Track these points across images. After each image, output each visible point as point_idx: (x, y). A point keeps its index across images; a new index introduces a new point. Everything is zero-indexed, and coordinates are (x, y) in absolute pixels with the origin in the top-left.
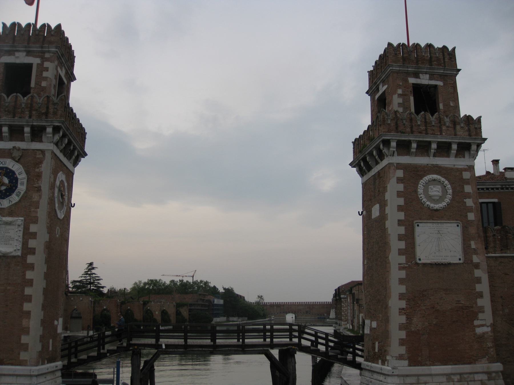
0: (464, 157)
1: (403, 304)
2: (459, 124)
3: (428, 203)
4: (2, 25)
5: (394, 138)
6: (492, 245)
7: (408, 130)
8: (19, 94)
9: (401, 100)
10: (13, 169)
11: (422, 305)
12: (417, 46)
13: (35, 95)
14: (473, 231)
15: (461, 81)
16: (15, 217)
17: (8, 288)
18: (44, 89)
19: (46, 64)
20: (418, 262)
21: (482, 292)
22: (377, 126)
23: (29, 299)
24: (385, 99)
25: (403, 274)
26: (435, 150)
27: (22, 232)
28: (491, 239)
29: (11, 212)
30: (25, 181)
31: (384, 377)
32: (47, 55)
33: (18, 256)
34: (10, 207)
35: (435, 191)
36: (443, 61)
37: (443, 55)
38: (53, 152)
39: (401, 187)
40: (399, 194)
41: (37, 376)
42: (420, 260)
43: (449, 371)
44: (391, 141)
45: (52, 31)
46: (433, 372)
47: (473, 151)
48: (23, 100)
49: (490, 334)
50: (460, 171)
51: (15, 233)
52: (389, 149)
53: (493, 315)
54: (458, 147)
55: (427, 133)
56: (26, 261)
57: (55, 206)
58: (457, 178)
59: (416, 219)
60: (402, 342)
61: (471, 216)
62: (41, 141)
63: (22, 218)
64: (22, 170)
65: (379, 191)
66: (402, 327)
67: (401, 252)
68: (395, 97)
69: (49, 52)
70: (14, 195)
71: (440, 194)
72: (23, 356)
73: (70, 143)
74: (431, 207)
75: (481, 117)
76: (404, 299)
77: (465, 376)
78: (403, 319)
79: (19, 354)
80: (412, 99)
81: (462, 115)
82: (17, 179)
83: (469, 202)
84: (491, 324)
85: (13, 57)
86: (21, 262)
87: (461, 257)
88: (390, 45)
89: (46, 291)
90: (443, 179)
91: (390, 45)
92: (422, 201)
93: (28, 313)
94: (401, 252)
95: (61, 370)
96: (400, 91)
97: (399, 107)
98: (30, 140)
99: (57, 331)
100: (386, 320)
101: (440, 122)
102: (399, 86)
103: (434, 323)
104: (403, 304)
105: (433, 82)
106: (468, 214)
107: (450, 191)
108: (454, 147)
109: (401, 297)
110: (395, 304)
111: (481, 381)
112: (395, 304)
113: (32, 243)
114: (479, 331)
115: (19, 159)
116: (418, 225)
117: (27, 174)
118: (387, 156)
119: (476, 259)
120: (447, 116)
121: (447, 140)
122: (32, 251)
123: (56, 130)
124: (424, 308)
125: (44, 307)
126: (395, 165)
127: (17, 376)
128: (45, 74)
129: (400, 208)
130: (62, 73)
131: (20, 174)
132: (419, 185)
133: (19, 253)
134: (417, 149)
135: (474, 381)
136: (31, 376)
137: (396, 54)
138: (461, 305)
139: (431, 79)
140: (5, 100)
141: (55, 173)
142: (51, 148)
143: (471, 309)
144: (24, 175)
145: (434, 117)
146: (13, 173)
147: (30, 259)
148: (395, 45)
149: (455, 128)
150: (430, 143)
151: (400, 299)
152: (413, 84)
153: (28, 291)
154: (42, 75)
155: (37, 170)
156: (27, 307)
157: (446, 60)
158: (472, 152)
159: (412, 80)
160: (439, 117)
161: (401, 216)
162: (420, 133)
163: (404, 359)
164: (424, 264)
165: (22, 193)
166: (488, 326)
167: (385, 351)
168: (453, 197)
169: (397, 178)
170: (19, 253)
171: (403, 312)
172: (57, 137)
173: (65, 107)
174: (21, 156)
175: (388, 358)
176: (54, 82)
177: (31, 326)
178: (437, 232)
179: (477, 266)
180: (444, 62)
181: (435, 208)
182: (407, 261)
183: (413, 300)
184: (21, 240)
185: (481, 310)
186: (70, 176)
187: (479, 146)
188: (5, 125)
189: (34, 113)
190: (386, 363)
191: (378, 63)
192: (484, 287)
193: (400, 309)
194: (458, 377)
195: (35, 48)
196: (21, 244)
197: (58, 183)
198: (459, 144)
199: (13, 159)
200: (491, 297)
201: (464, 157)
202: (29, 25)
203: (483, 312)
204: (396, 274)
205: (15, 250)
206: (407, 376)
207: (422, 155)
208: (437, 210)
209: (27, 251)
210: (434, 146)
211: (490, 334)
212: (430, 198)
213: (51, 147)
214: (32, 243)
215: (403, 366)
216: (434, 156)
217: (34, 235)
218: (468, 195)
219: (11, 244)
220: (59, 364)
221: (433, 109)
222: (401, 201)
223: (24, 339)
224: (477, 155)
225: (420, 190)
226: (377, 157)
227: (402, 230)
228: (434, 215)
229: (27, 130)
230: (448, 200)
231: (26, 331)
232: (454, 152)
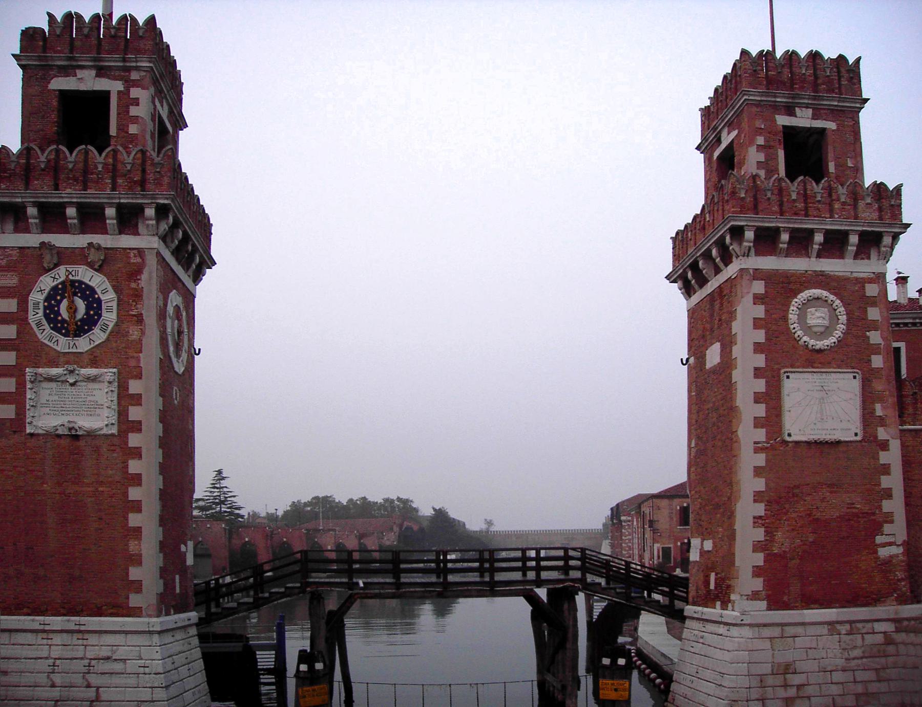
0: (869, 258)
1: (760, 509)
2: (863, 199)
3: (805, 338)
4: (47, 18)
5: (750, 223)
6: (911, 410)
7: (776, 208)
8: (90, 147)
9: (761, 157)
10: (90, 284)
11: (791, 510)
12: (791, 56)
13: (120, 148)
15: (868, 120)
16: (101, 367)
17: (100, 489)
20: (788, 439)
21: (890, 489)
22: (721, 203)
23: (137, 507)
24: (733, 156)
25: (760, 460)
26: (820, 244)
27: (115, 394)
28: (909, 400)
29: (94, 358)
30: (114, 304)
31: (727, 628)
32: (134, 76)
33: (113, 435)
34: (91, 351)
36: (834, 82)
37: (839, 72)
38: (158, 254)
39: (760, 311)
40: (757, 324)
41: (159, 633)
42: (789, 435)
43: (834, 619)
44: (746, 228)
45: (139, 28)
46: (807, 620)
47: (885, 247)
48: (99, 159)
49: (901, 558)
50: (862, 282)
52: (740, 244)
53: (907, 528)
54: (859, 240)
55: (806, 215)
56: (126, 443)
57: (168, 350)
58: (855, 296)
59: (787, 367)
60: (757, 572)
61: (877, 361)
62: (136, 233)
63: (115, 370)
64: (108, 285)
65: (720, 320)
66: (758, 547)
67: (758, 423)
68: (752, 150)
69: (137, 68)
70: (96, 330)
71: (826, 323)
72: (135, 600)
74: (810, 346)
75: (901, 185)
76: (761, 502)
77: (860, 625)
78: (760, 534)
79: (128, 598)
80: (781, 154)
81: (868, 182)
82: (99, 301)
83: (875, 337)
84: (904, 541)
85: (72, 79)
86: (119, 443)
87: (858, 431)
88: (744, 53)
89: (163, 494)
90: (832, 297)
91: (744, 53)
92: (796, 335)
93: (138, 530)
94: (758, 423)
95: (197, 625)
96: (760, 140)
97: (758, 168)
98: (117, 231)
99: (185, 562)
100: (732, 537)
101: (830, 195)
102: (759, 132)
103: (811, 540)
104: (760, 509)
105: (818, 124)
106: (873, 356)
107: (843, 318)
108: (854, 239)
109: (758, 497)
110: (747, 510)
111: (884, 633)
112: (747, 510)
113: (134, 413)
114: (883, 552)
115: (100, 266)
116: (788, 377)
117: (116, 292)
118: (737, 257)
119: (882, 434)
120: (842, 185)
121: (843, 228)
122: (137, 427)
123: (162, 211)
124: (794, 515)
125: (162, 521)
126: (751, 272)
127: (126, 633)
128: (134, 111)
129: (758, 348)
131: (105, 292)
132: (792, 308)
133: (114, 430)
134: (789, 243)
135: (874, 633)
136: (150, 633)
137: (755, 71)
138: (854, 510)
139: (815, 117)
140: (66, 158)
141: (164, 291)
142: (156, 246)
143: (873, 517)
144: (111, 295)
145: (821, 185)
146: (93, 290)
147: (134, 440)
148: (754, 53)
149: (855, 206)
150: (811, 232)
151: (755, 501)
152: (784, 126)
153: (134, 493)
154: (128, 112)
155: (133, 285)
156: (134, 520)
157: (844, 82)
158: (883, 249)
159: (783, 120)
160: (830, 186)
161: (760, 361)
162: (796, 214)
163: (759, 599)
164: (797, 443)
165: (111, 325)
166: (898, 545)
167: (729, 587)
168: (848, 329)
169: (754, 294)
170: (114, 430)
171: (760, 521)
172: (164, 227)
173: (175, 170)
174: (103, 261)
175: (733, 597)
176: (150, 126)
177: (144, 552)
178: (820, 388)
179: (884, 446)
180: (840, 84)
181: (817, 347)
182: (769, 436)
183: (778, 503)
184: (116, 407)
185: (889, 518)
187: (895, 237)
188: (71, 204)
190: (730, 605)
191: (720, 91)
192: (894, 481)
193: (754, 518)
194: (847, 627)
195: (113, 61)
196: (116, 414)
198: (862, 235)
199: (91, 265)
200: (906, 497)
201: (869, 258)
202: (96, 17)
203: (892, 522)
204: (749, 459)
205: (107, 425)
206: (765, 625)
208: (820, 351)
209: (127, 426)
210: (819, 238)
211: (901, 558)
212: (808, 329)
213: (155, 243)
214: (134, 413)
215: (759, 610)
216: (819, 256)
217: (137, 400)
218: (874, 326)
219: (99, 415)
220: (193, 616)
221: (817, 172)
222: (760, 336)
223: (134, 573)
224: (891, 255)
225: (793, 317)
226: (718, 260)
227: (760, 385)
228: (815, 360)
229: (110, 212)
230: (840, 334)
231: (137, 560)
232: (852, 249)
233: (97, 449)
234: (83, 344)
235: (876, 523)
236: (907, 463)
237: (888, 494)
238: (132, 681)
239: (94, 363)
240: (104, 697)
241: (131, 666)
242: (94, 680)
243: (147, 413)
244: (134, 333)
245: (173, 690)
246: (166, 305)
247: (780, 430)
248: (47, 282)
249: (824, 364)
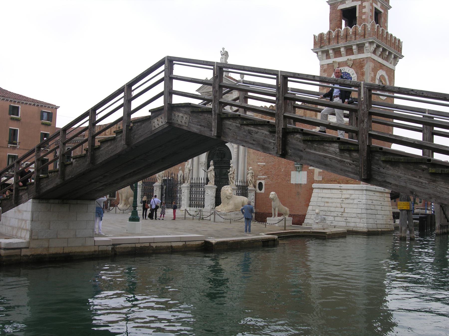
18: (364, 20)
62: (363, 53)
73: (384, 50)
85: (345, 4)
136: (362, 190)
142: (369, 56)
146: (349, 74)
189: (357, 36)
197: (378, 77)
199: (349, 66)
238: (355, 206)
240: (346, 211)
241: (356, 201)
242: (344, 205)
245: (369, 211)
246: (375, 76)
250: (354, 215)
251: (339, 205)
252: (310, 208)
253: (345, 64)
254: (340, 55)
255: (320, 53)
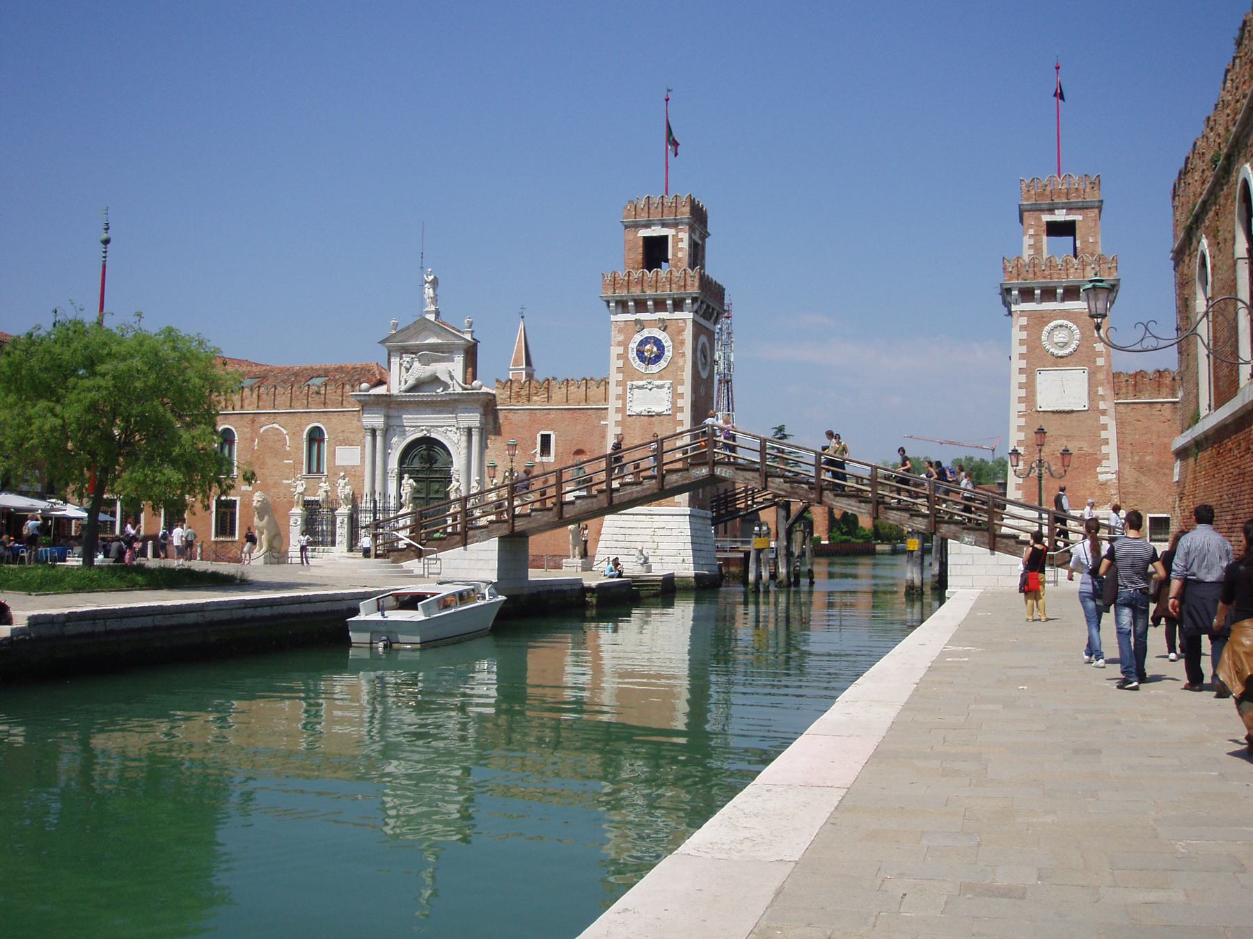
6: (1124, 391)
14: (1101, 376)
18: (680, 260)
19: (681, 235)
35: (1059, 337)
39: (1024, 335)
51: (665, 394)
73: (708, 306)
86: (672, 416)
90: (1070, 324)
94: (1020, 400)
113: (680, 403)
114: (1102, 478)
119: (1102, 406)
122: (681, 409)
123: (694, 300)
128: (680, 245)
129: (1022, 356)
130: (696, 238)
147: (679, 416)
161: (1023, 364)
172: (696, 306)
179: (1104, 412)
185: (1106, 457)
186: (710, 335)
192: (1111, 434)
207: (1049, 300)
210: (1060, 291)
213: (691, 315)
216: (1063, 300)
225: (1044, 338)
228: (1059, 361)
233: (661, 422)
234: (655, 369)
235: (1095, 461)
236: (1121, 424)
237: (1106, 442)
238: (675, 539)
239: (660, 378)
241: (675, 532)
242: (656, 539)
243: (686, 403)
244: (681, 362)
247: (1035, 405)
248: (638, 338)
249: (1064, 365)
250: (675, 553)
251: (648, 538)
252: (601, 544)
253: (652, 324)
254: (646, 310)
255: (612, 304)
